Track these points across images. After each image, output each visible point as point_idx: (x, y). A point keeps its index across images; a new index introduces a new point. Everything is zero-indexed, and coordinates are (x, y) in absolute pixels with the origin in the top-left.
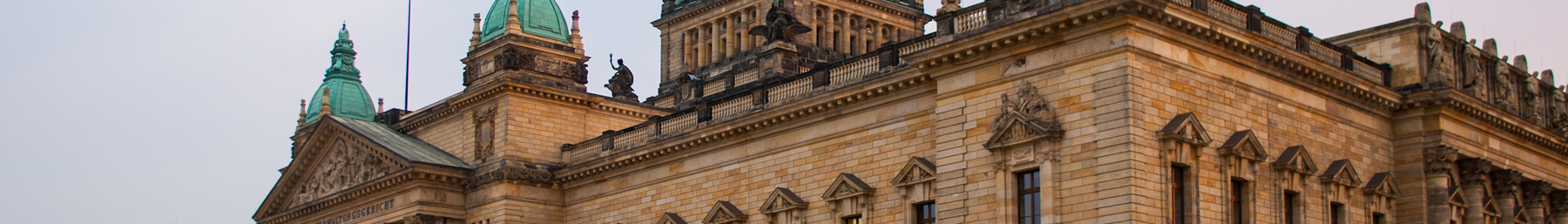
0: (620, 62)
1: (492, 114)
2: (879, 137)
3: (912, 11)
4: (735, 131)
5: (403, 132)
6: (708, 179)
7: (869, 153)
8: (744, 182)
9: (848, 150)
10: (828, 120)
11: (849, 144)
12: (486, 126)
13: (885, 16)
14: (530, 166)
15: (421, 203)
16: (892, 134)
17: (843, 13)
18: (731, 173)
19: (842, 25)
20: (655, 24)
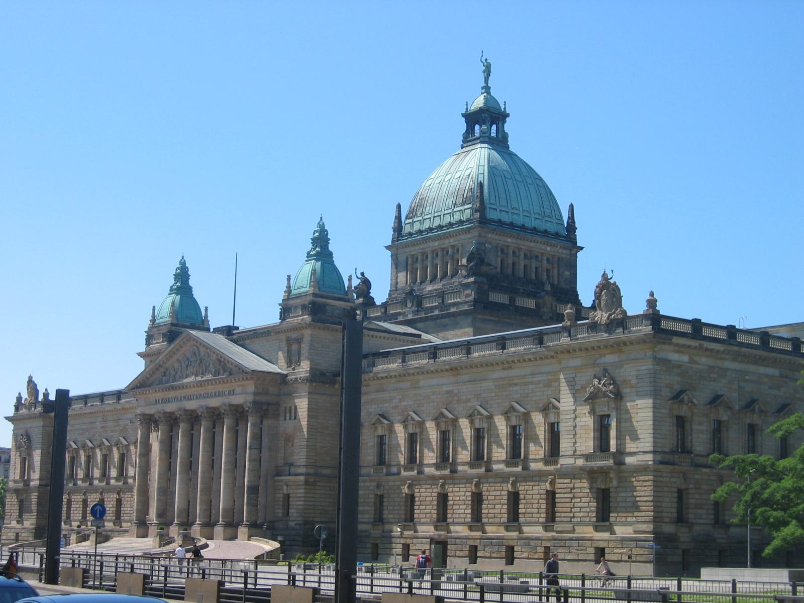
0: (362, 274)
1: (299, 341)
2: (532, 383)
3: (569, 244)
4: (451, 369)
5: (235, 342)
6: (434, 393)
7: (526, 391)
8: (456, 398)
9: (515, 388)
10: (504, 369)
11: (516, 385)
12: (295, 347)
13: (548, 249)
14: (323, 374)
15: (255, 394)
16: (539, 382)
17: (519, 249)
18: (448, 392)
19: (519, 256)
20: (387, 248)
